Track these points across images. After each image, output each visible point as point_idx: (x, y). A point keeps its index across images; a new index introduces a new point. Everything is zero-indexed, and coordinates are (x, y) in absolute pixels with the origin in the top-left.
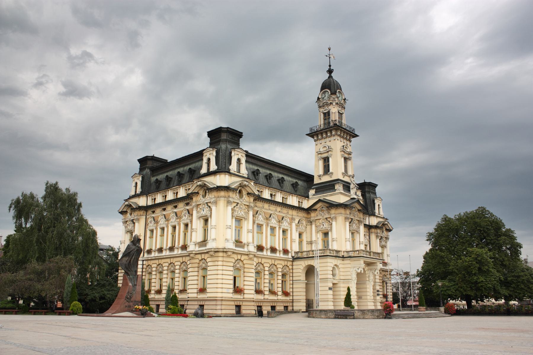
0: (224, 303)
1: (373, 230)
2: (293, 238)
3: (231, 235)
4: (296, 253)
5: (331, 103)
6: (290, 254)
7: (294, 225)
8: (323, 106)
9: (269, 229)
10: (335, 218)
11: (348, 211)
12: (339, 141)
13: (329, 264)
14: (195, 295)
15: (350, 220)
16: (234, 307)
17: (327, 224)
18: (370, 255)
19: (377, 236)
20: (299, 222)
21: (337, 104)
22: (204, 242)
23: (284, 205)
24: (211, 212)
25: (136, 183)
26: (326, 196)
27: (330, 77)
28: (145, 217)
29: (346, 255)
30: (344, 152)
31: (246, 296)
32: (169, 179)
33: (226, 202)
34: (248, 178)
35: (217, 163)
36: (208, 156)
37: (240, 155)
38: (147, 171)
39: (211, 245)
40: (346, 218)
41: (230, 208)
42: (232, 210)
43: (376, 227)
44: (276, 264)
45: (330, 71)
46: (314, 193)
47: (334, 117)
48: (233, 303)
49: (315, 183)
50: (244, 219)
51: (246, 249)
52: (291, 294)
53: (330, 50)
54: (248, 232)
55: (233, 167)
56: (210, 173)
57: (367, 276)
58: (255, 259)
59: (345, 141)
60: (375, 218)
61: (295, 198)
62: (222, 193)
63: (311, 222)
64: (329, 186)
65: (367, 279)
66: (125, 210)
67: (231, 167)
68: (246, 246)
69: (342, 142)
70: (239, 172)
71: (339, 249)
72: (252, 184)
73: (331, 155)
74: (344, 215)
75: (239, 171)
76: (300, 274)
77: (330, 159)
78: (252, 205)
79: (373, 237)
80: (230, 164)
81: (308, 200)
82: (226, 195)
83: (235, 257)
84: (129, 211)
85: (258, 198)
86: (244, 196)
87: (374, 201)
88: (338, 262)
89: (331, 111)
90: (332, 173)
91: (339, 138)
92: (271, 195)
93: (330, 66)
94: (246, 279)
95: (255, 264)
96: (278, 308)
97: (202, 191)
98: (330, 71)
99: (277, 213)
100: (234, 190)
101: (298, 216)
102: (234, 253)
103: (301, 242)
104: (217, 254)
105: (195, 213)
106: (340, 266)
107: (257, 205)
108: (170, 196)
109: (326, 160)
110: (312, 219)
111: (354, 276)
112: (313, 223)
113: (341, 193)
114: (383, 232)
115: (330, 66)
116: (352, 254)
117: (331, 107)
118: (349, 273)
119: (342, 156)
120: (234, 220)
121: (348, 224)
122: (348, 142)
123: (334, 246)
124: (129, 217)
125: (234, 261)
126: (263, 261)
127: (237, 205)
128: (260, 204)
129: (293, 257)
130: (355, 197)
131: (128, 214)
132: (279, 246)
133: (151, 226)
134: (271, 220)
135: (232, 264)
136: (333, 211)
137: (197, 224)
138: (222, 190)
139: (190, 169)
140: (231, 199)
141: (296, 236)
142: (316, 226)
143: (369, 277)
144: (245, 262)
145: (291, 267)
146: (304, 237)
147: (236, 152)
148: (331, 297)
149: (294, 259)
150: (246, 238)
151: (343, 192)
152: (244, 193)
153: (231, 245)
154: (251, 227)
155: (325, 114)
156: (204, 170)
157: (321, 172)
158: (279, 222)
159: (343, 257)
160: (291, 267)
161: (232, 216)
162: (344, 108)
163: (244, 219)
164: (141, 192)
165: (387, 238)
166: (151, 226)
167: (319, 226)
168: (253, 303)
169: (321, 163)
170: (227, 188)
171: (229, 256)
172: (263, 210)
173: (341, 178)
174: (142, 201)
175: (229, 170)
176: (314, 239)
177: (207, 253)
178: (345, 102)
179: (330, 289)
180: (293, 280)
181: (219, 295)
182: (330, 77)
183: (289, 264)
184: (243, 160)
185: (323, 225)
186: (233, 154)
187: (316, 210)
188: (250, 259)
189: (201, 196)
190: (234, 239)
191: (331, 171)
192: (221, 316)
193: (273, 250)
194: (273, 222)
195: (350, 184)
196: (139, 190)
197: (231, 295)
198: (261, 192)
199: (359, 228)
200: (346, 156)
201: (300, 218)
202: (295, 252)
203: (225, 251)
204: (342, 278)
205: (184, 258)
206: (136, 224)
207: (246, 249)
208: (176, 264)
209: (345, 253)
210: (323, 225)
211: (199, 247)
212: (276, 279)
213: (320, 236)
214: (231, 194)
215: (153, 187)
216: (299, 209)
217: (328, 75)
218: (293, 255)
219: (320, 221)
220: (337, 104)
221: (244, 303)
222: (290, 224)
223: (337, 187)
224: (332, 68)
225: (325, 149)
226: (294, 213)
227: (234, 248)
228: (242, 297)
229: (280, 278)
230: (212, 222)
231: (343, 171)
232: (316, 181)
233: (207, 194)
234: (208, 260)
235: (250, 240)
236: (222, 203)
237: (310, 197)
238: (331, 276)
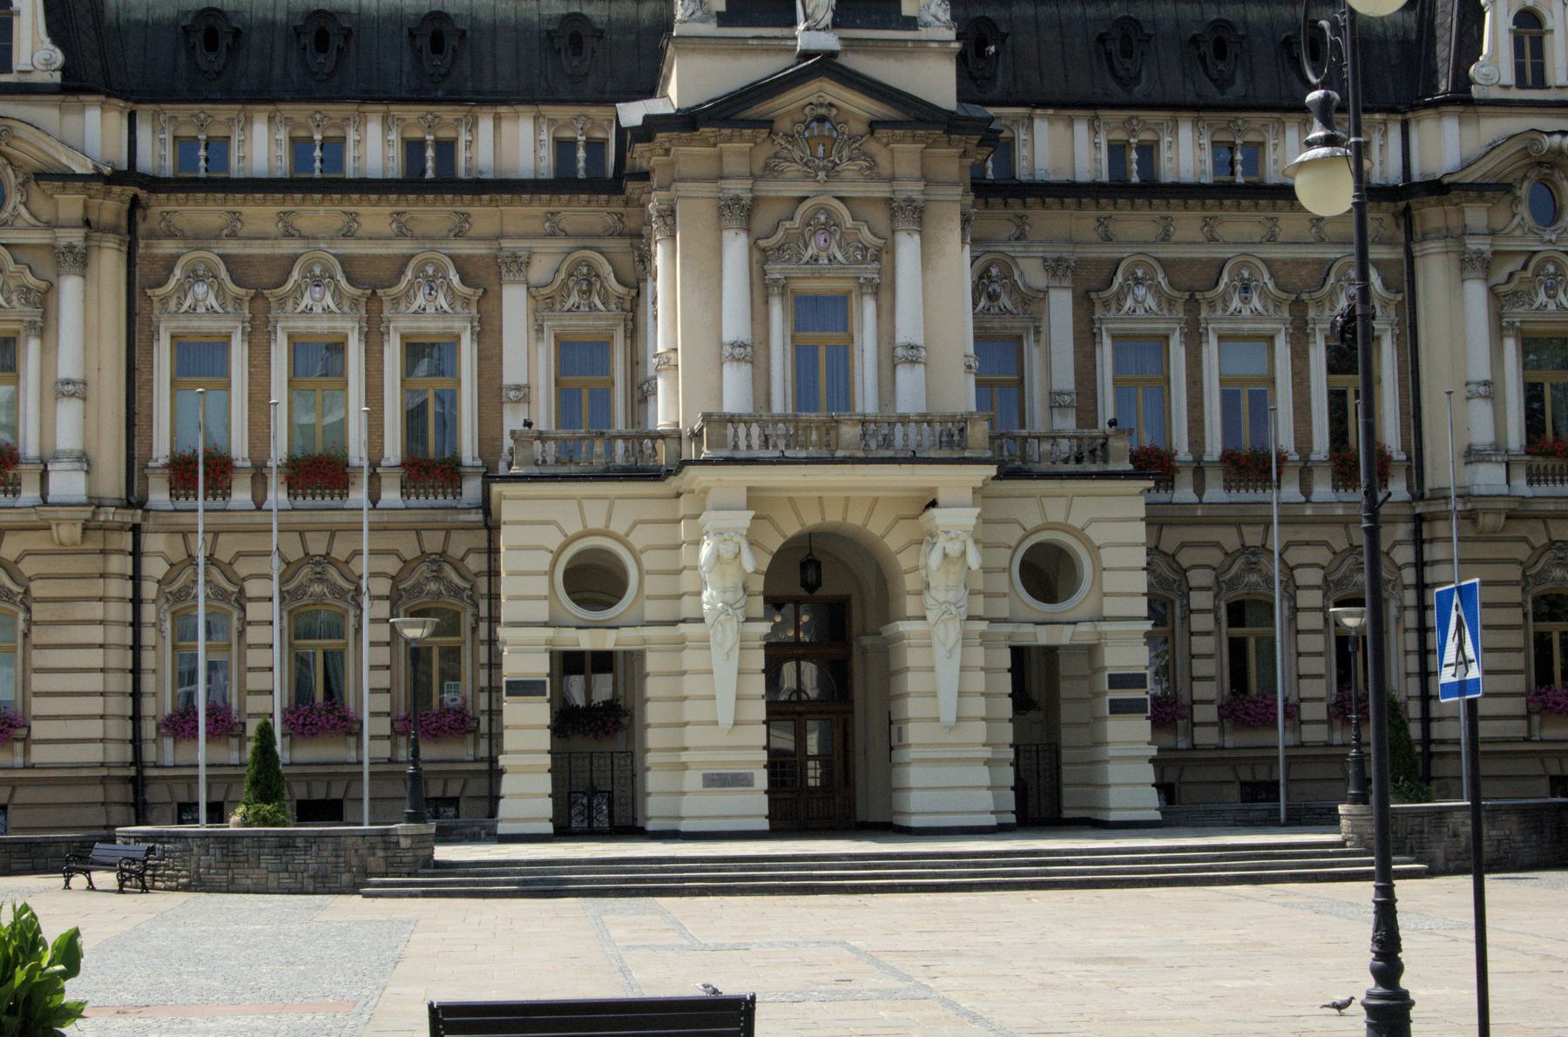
1: (1432, 215)
2: (513, 372)
7: (514, 302)
10: (669, 214)
19: (1468, 263)
31: (39, 754)
43: (1438, 188)
52: (484, 727)
57: (910, 582)
74: (706, 189)
79: (1434, 270)
94: (40, 658)
106: (639, 539)
107: (179, 221)
121: (736, 248)
145: (476, 563)
194: (319, 311)
199: (884, 254)
204: (653, 611)
207: (29, 494)
221: (22, 796)
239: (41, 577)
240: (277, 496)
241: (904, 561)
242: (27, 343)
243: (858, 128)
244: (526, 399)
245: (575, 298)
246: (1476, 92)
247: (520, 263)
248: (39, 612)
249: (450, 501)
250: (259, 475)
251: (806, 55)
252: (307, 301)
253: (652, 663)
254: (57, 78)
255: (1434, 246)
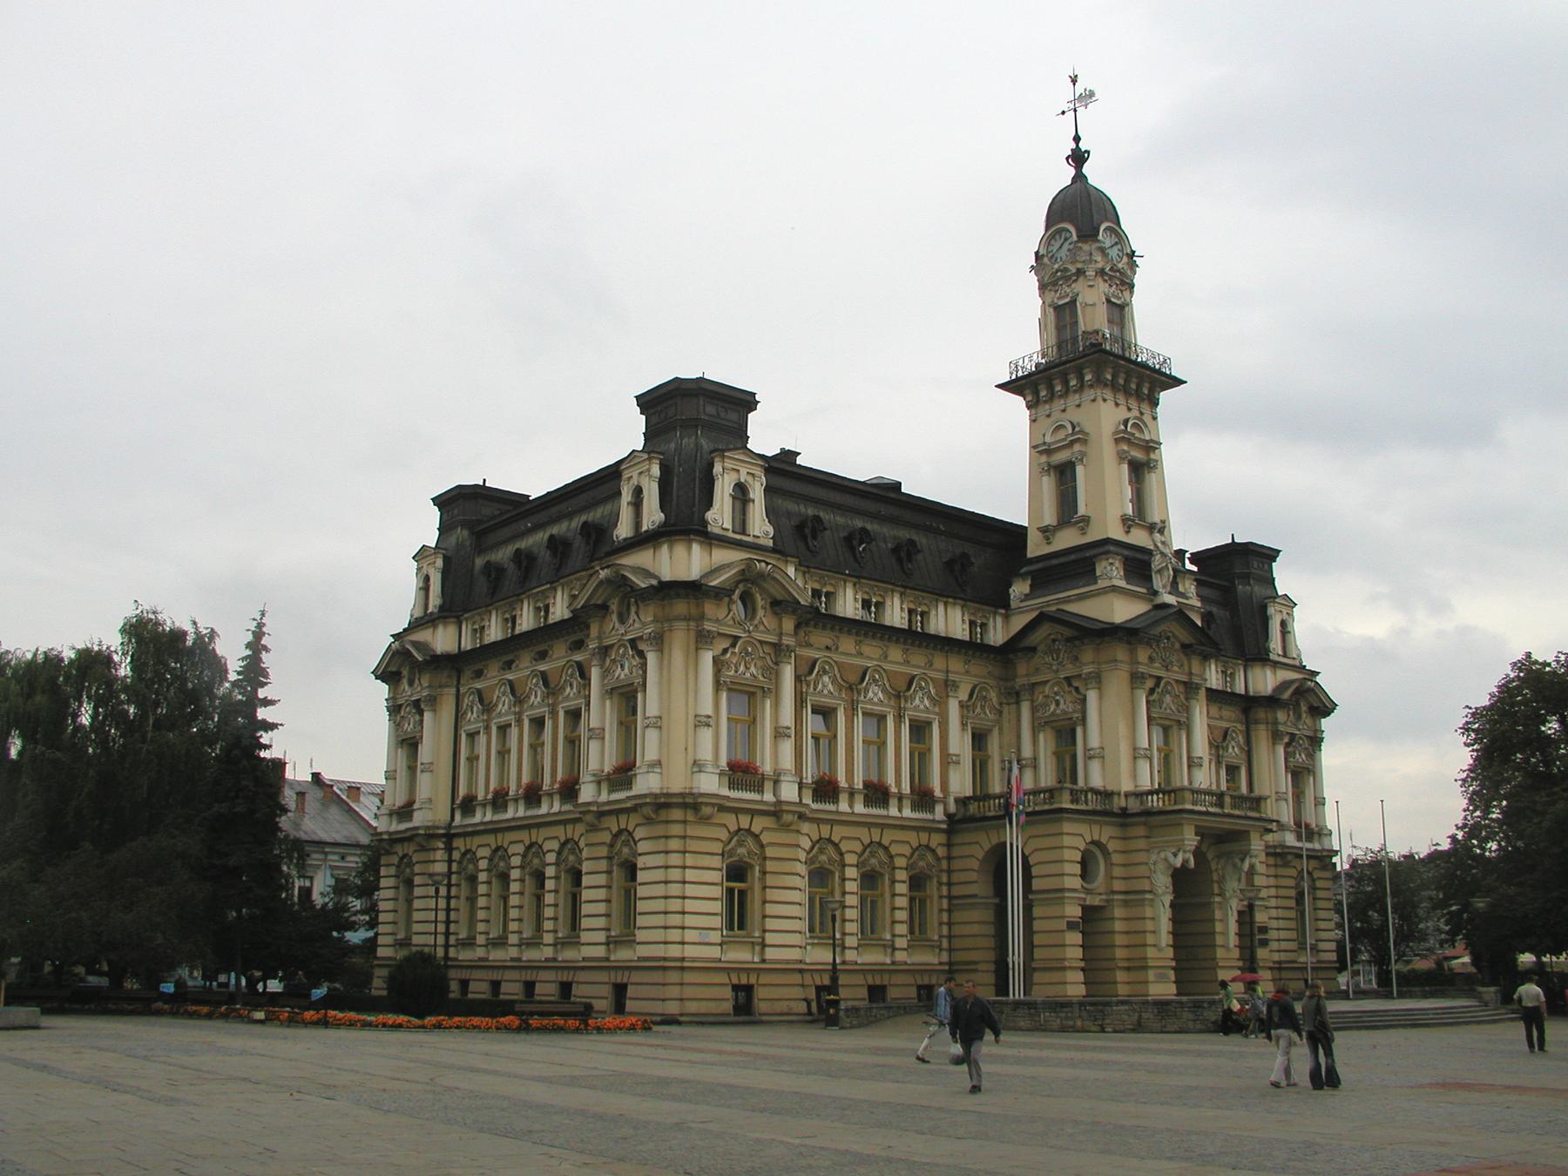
0: (689, 977)
2: (954, 748)
3: (713, 747)
4: (963, 802)
5: (1080, 272)
6: (939, 809)
8: (1055, 284)
9: (859, 720)
11: (1143, 655)
12: (1110, 403)
13: (1067, 841)
14: (600, 951)
15: (1150, 684)
16: (728, 993)
17: (1069, 699)
18: (1221, 806)
19: (1276, 736)
20: (971, 696)
21: (1101, 272)
22: (623, 774)
23: (915, 638)
24: (645, 672)
25: (427, 579)
26: (1068, 600)
27: (1079, 177)
28: (453, 691)
29: (1134, 805)
30: (1129, 442)
31: (770, 954)
32: (525, 561)
33: (692, 634)
34: (774, 550)
35: (664, 503)
36: (634, 481)
37: (743, 472)
38: (461, 534)
39: (646, 783)
40: (1136, 678)
41: (707, 658)
42: (716, 661)
43: (1272, 701)
44: (885, 842)
45: (1078, 158)
46: (1027, 589)
47: (1094, 318)
48: (722, 978)
49: (1029, 555)
50: (759, 694)
51: (768, 797)
53: (1074, 81)
54: (779, 734)
55: (720, 515)
56: (643, 540)
58: (806, 827)
59: (1133, 403)
60: (1268, 672)
61: (958, 613)
62: (680, 607)
63: (1018, 694)
64: (1077, 566)
65: (1216, 891)
66: (393, 669)
67: (709, 515)
68: (768, 786)
69: (1123, 408)
70: (744, 532)
71: (1109, 788)
72: (791, 571)
73: (1083, 454)
75: (741, 524)
76: (974, 876)
77: (1079, 470)
78: (788, 641)
79: (1262, 736)
80: (709, 505)
81: (1006, 617)
82: (694, 611)
83: (730, 820)
84: (405, 673)
85: (816, 618)
86: (760, 613)
87: (1264, 608)
88: (1105, 833)
89: (1080, 299)
90: (1086, 520)
91: (1108, 394)
92: (866, 604)
93: (1077, 139)
95: (806, 844)
96: (893, 993)
97: (616, 601)
98: (1078, 158)
99: (887, 666)
100: (720, 594)
101: (967, 672)
102: (722, 809)
103: (980, 768)
104: (663, 815)
105: (595, 674)
108: (527, 620)
109: (1064, 474)
110: (1020, 681)
111: (1163, 882)
112: (1025, 696)
113: (1114, 589)
114: (1299, 717)
115: (1077, 139)
116: (1155, 802)
117: (1079, 286)
118: (1142, 870)
119: (1121, 457)
120: (724, 695)
122: (1145, 407)
123: (1095, 777)
124: (408, 692)
125: (724, 835)
126: (838, 833)
127: (733, 645)
128: (821, 638)
129: (949, 816)
130: (1171, 599)
131: (405, 684)
132: (898, 778)
133: (473, 717)
134: (866, 691)
135: (717, 847)
136: (1088, 655)
137: (601, 713)
138: (678, 596)
139: (585, 523)
140: (708, 626)
141: (960, 743)
142: (1034, 710)
143: (1221, 881)
144: (765, 838)
145: (941, 852)
146: (994, 746)
147: (729, 464)
148: (1079, 953)
149: (956, 824)
150: (777, 756)
151: (1123, 584)
152: (760, 602)
153: (710, 783)
154: (787, 718)
155: (1058, 309)
156: (623, 530)
157: (1049, 518)
158: (898, 697)
159: (1124, 813)
160: (941, 852)
161: (718, 685)
162: (1132, 286)
163: (759, 694)
164: (442, 608)
165: (1316, 741)
166: (473, 717)
167: (1046, 705)
168: (797, 978)
169: (1048, 484)
170: (693, 590)
171: (705, 820)
172: (836, 657)
173: (1116, 533)
174: (443, 640)
175: (705, 523)
176: (1027, 752)
177: (634, 809)
178: (1133, 265)
179: (1071, 926)
180: (950, 897)
181: (674, 951)
182: (1079, 177)
183: (937, 840)
184: (757, 492)
185: (1058, 704)
186: (717, 468)
187: (1033, 649)
188: (785, 827)
189: (614, 617)
190: (723, 762)
191: (1082, 510)
192: (679, 1023)
193: (877, 793)
195: (1149, 552)
196: (435, 600)
197: (715, 952)
198: (828, 595)
199: (1188, 709)
200: (1138, 455)
201: (975, 680)
202: (957, 800)
203: (691, 803)
205: (623, 818)
206: (427, 716)
208: (546, 846)
209: (1131, 800)
210: (1058, 704)
211: (610, 792)
212: (887, 895)
213: (1046, 743)
214: (710, 608)
215: (482, 585)
216: (972, 648)
217: (1072, 172)
218: (952, 808)
219: (1047, 689)
220: (1101, 272)
221: (764, 979)
222: (940, 702)
223: (1100, 568)
224: (1083, 146)
225: (1061, 435)
226: (956, 664)
227: (725, 792)
228: (756, 959)
229: (902, 888)
230: (651, 703)
231: (1129, 510)
232: (1035, 547)
233: (633, 609)
234: (637, 835)
235: (787, 761)
236: (679, 639)
237: (1013, 605)
238: (1076, 883)
239: (771, 844)
240: (859, 808)
241: (1213, 866)
242: (763, 703)
243: (1177, 646)
244: (958, 763)
245: (978, 710)
246: (1272, 656)
247: (955, 686)
248: (770, 866)
249: (929, 816)
250: (852, 793)
251: (1165, 606)
252: (870, 694)
253: (1118, 912)
254: (770, 543)
255: (1262, 727)
